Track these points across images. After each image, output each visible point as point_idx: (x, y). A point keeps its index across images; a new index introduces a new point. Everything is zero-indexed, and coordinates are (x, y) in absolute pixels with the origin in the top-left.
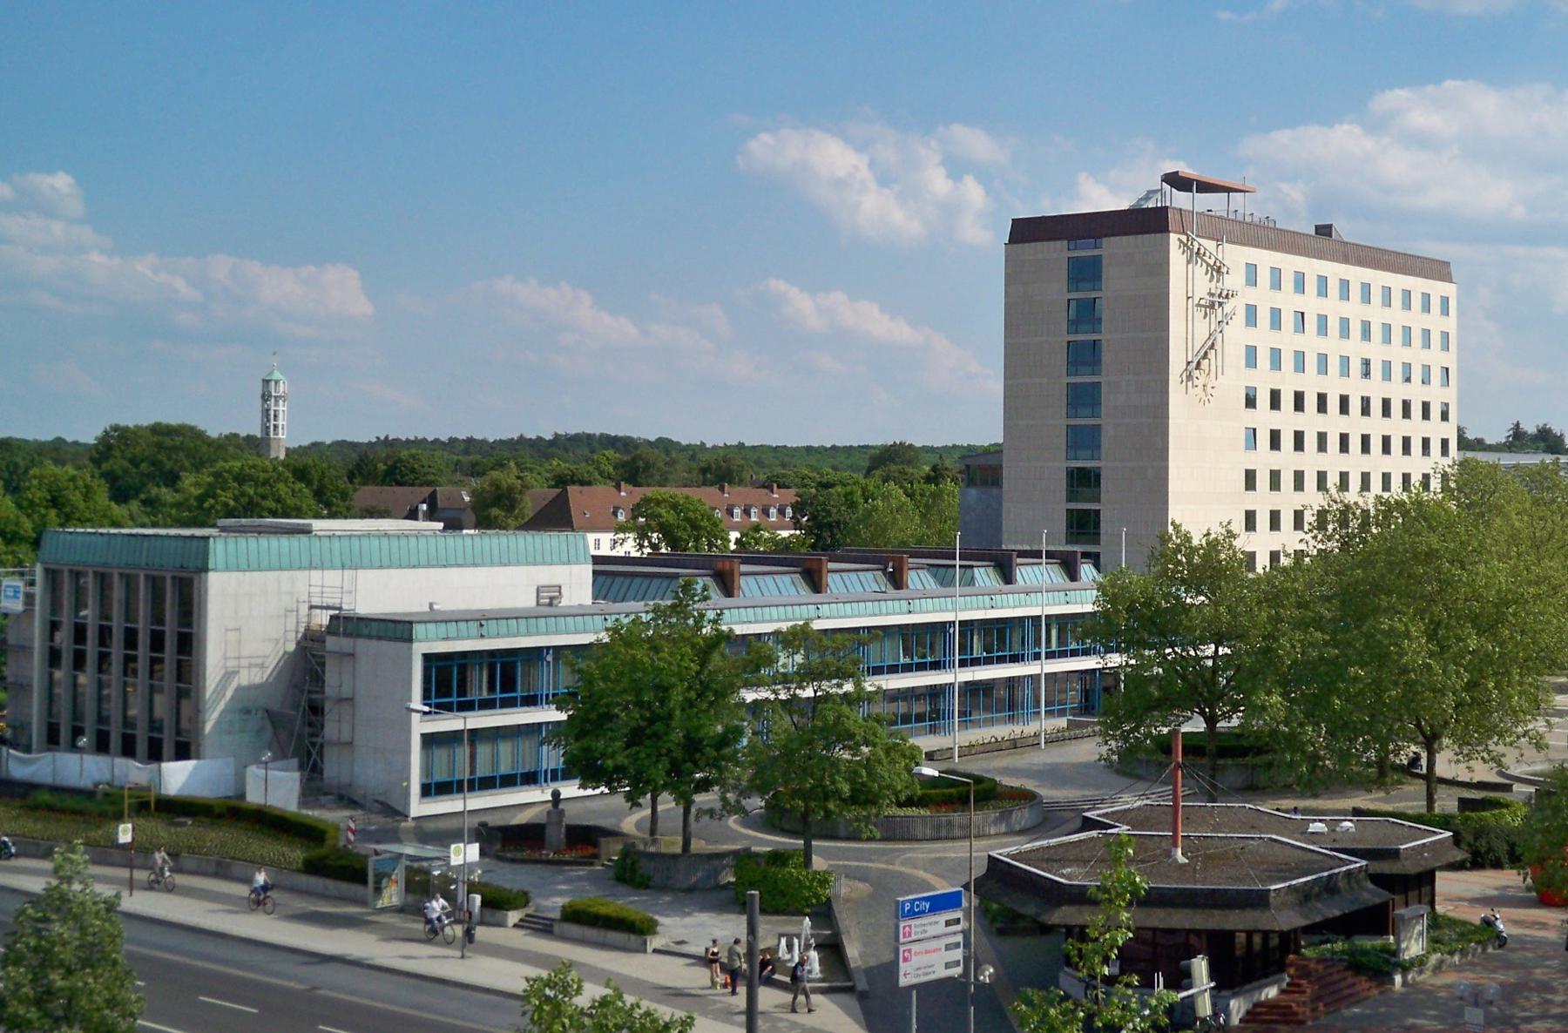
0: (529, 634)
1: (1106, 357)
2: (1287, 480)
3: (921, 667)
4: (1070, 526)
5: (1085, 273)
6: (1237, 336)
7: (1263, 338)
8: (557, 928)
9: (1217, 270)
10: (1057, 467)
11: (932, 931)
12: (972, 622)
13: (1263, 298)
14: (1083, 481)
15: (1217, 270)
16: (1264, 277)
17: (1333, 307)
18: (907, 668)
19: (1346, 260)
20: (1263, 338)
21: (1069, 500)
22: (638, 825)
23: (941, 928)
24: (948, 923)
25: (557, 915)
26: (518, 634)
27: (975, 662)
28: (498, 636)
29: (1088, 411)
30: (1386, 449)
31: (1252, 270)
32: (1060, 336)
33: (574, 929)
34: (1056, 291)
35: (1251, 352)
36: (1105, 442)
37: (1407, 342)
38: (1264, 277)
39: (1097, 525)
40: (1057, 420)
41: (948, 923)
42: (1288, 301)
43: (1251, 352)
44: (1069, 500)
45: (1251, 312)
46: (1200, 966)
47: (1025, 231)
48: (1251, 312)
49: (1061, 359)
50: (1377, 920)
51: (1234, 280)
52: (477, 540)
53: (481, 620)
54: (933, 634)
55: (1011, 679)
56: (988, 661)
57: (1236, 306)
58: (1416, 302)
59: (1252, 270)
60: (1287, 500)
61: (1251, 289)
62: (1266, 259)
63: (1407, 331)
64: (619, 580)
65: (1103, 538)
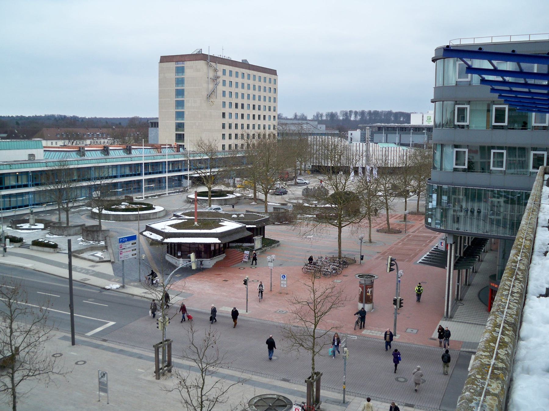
0: (24, 168)
1: (186, 93)
2: (233, 126)
3: (135, 175)
4: (176, 138)
5: (180, 70)
6: (220, 88)
7: (227, 89)
8: (31, 247)
9: (216, 70)
10: (173, 122)
11: (128, 246)
12: (148, 163)
13: (227, 78)
14: (180, 126)
15: (216, 70)
16: (227, 73)
17: (240, 80)
18: (131, 175)
19: (249, 69)
20: (227, 89)
21: (176, 131)
22: (56, 219)
23: (130, 245)
24: (132, 244)
25: (31, 243)
26: (21, 168)
27: (150, 174)
28: (15, 168)
29: (181, 108)
30: (259, 118)
31: (224, 71)
32: (173, 88)
33: (35, 248)
34: (172, 76)
35: (224, 92)
36: (185, 116)
37: (265, 91)
38: (227, 73)
39: (184, 138)
40: (173, 110)
41: (132, 244)
42: (234, 79)
43: (224, 92)
44: (176, 131)
45: (224, 81)
46: (192, 255)
47: (164, 59)
48: (224, 81)
49: (174, 93)
50: (250, 240)
51: (220, 73)
52: (10, 143)
53: (10, 165)
54: (138, 166)
55: (159, 178)
56: (153, 173)
57: (220, 80)
58: (268, 80)
59: (224, 71)
60: (233, 131)
61: (224, 76)
62: (228, 68)
63: (243, 84)
64: (52, 153)
65: (185, 141)
